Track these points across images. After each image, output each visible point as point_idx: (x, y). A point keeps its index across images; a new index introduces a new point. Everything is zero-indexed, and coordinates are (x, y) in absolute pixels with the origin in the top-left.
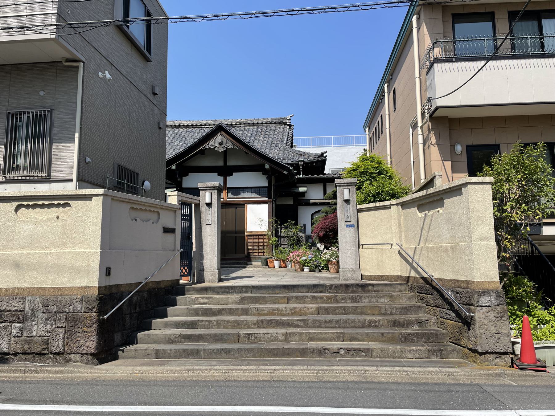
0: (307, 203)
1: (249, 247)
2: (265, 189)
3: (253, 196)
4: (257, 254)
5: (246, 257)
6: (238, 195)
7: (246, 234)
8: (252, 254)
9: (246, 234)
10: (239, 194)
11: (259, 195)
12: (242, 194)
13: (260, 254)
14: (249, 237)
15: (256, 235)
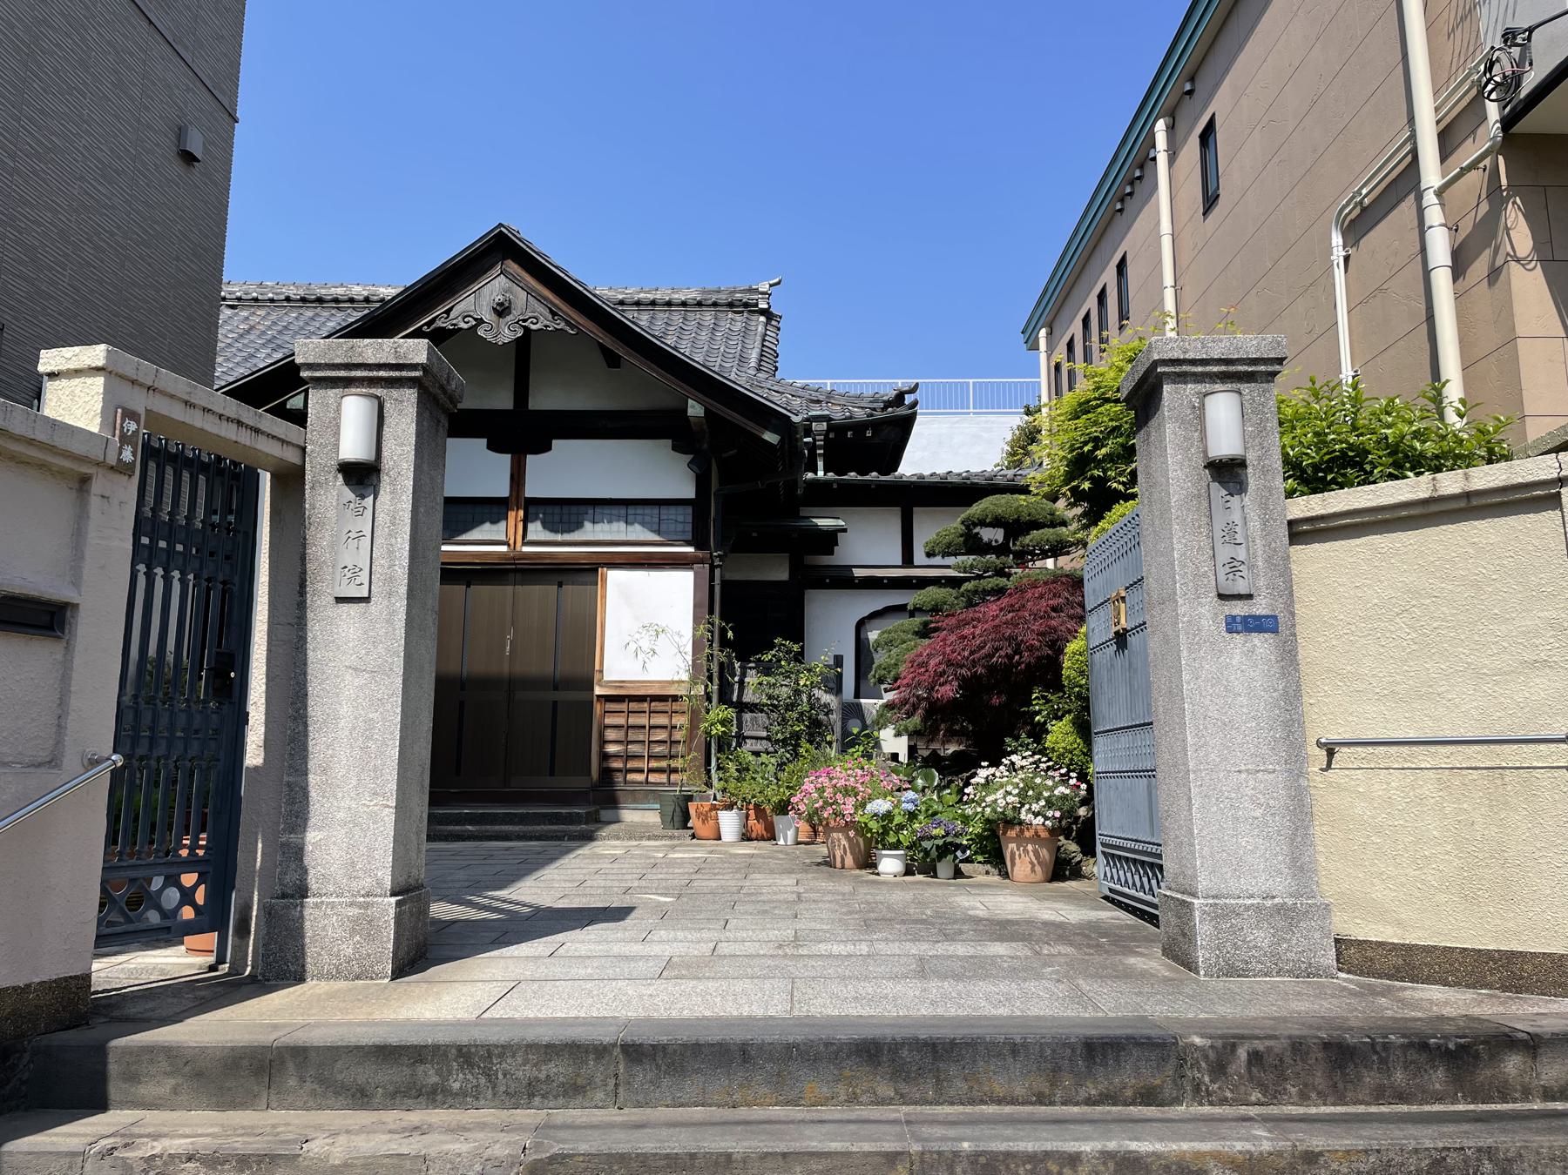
0: (844, 580)
1: (612, 749)
2: (680, 509)
4: (640, 777)
5: (594, 788)
6: (570, 531)
7: (598, 691)
8: (619, 778)
9: (598, 691)
10: (579, 526)
11: (658, 532)
12: (588, 525)
13: (653, 778)
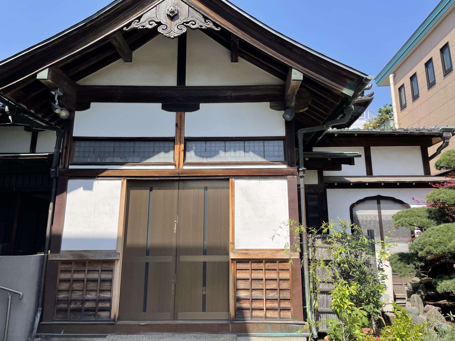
0: (344, 185)
1: (242, 294)
2: (276, 143)
3: (248, 160)
4: (261, 314)
5: (231, 320)
6: (211, 157)
7: (232, 256)
8: (248, 314)
9: (232, 256)
10: (216, 153)
11: (264, 157)
12: (222, 153)
13: (270, 314)
14: (240, 266)
15: (259, 261)
